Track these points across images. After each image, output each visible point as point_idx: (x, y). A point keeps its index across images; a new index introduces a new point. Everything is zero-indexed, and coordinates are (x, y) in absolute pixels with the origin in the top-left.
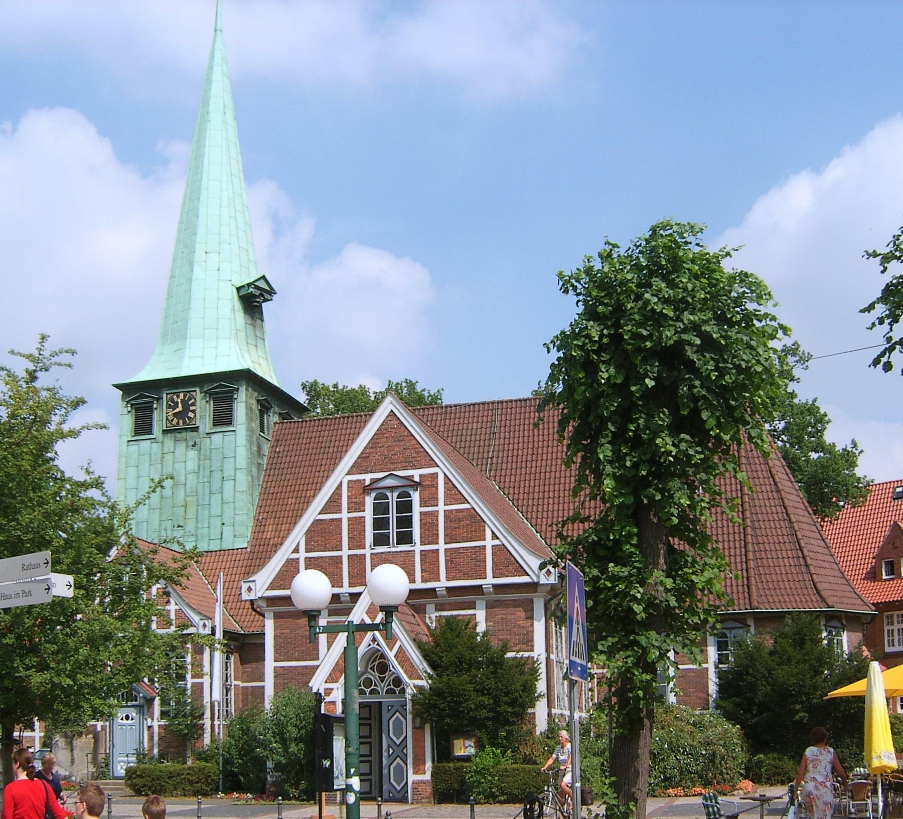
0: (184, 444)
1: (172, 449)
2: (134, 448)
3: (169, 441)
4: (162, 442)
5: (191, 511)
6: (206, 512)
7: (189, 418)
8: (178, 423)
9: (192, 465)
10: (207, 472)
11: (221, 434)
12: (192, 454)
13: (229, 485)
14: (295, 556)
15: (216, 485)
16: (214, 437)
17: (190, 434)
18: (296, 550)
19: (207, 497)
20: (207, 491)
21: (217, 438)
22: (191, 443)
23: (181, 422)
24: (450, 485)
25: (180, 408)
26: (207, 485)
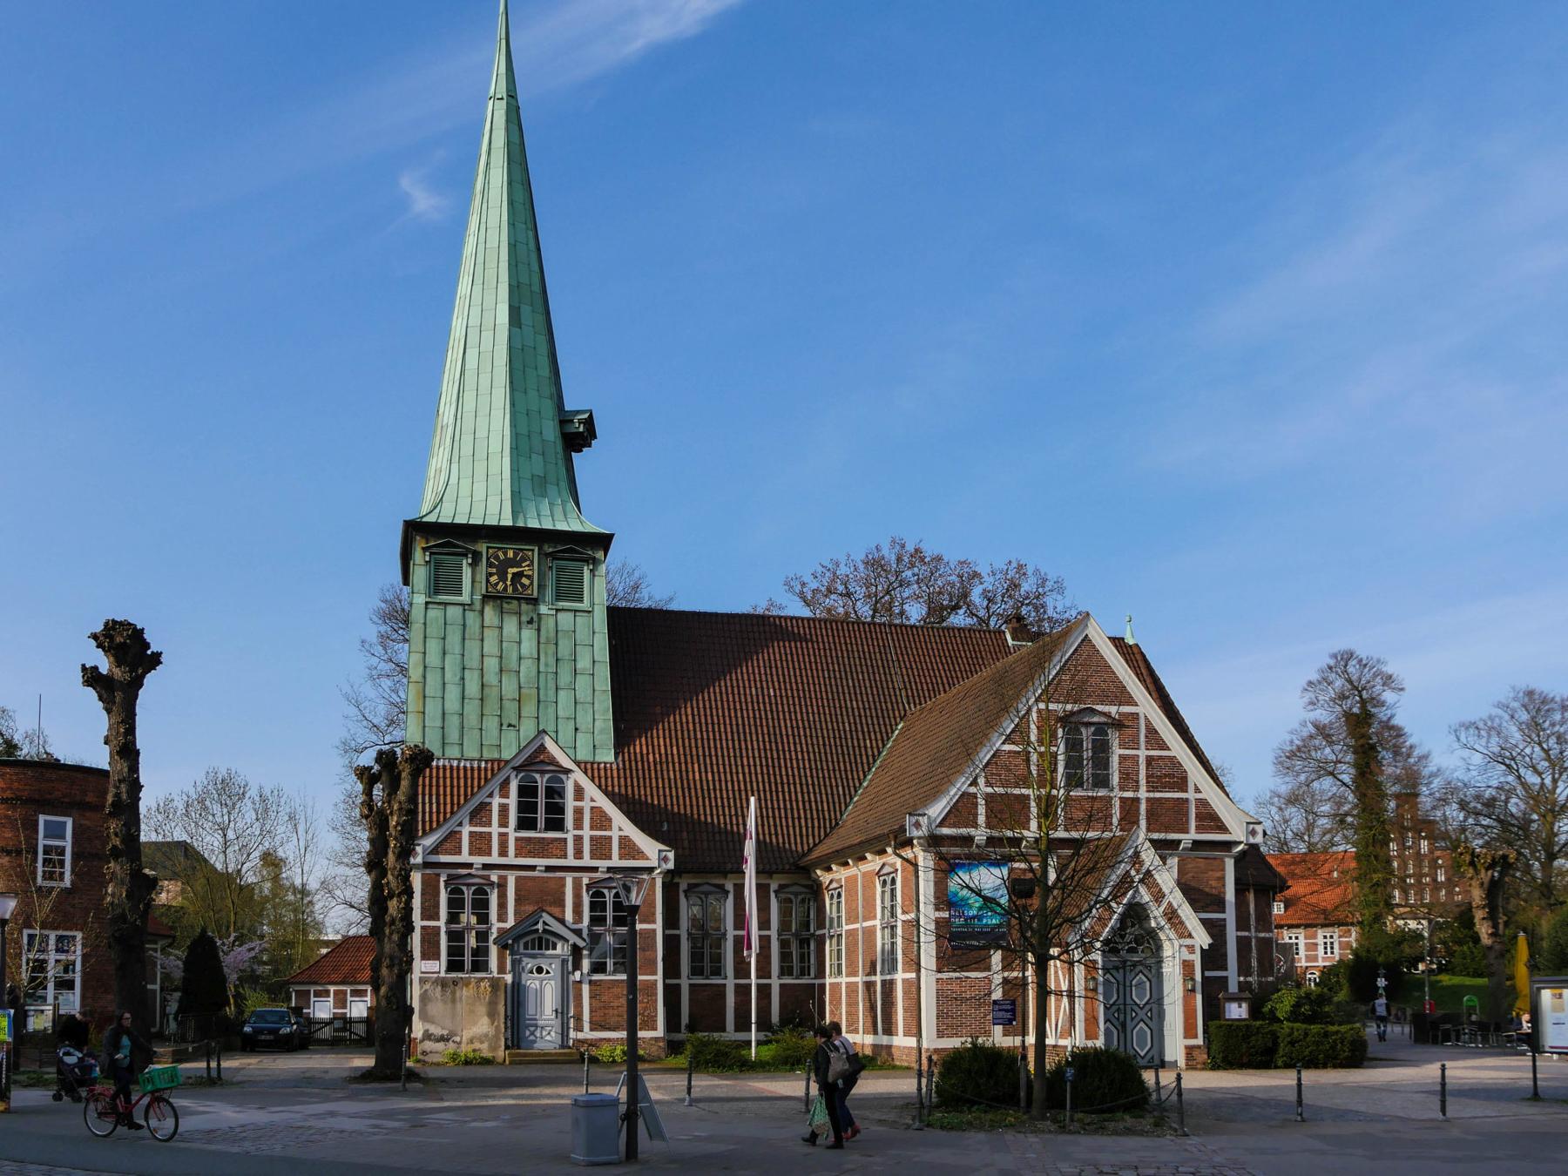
0: (514, 619)
1: (496, 622)
2: (434, 613)
3: (490, 613)
4: (482, 612)
5: (529, 709)
6: (551, 710)
7: (523, 586)
8: (505, 589)
9: (528, 647)
10: (552, 661)
11: (571, 615)
12: (528, 634)
13: (583, 682)
14: (973, 790)
15: (565, 678)
16: (560, 615)
17: (524, 607)
18: (974, 783)
19: (552, 693)
20: (551, 685)
21: (565, 619)
22: (524, 618)
23: (510, 590)
24: (1152, 732)
25: (512, 571)
26: (550, 677)
